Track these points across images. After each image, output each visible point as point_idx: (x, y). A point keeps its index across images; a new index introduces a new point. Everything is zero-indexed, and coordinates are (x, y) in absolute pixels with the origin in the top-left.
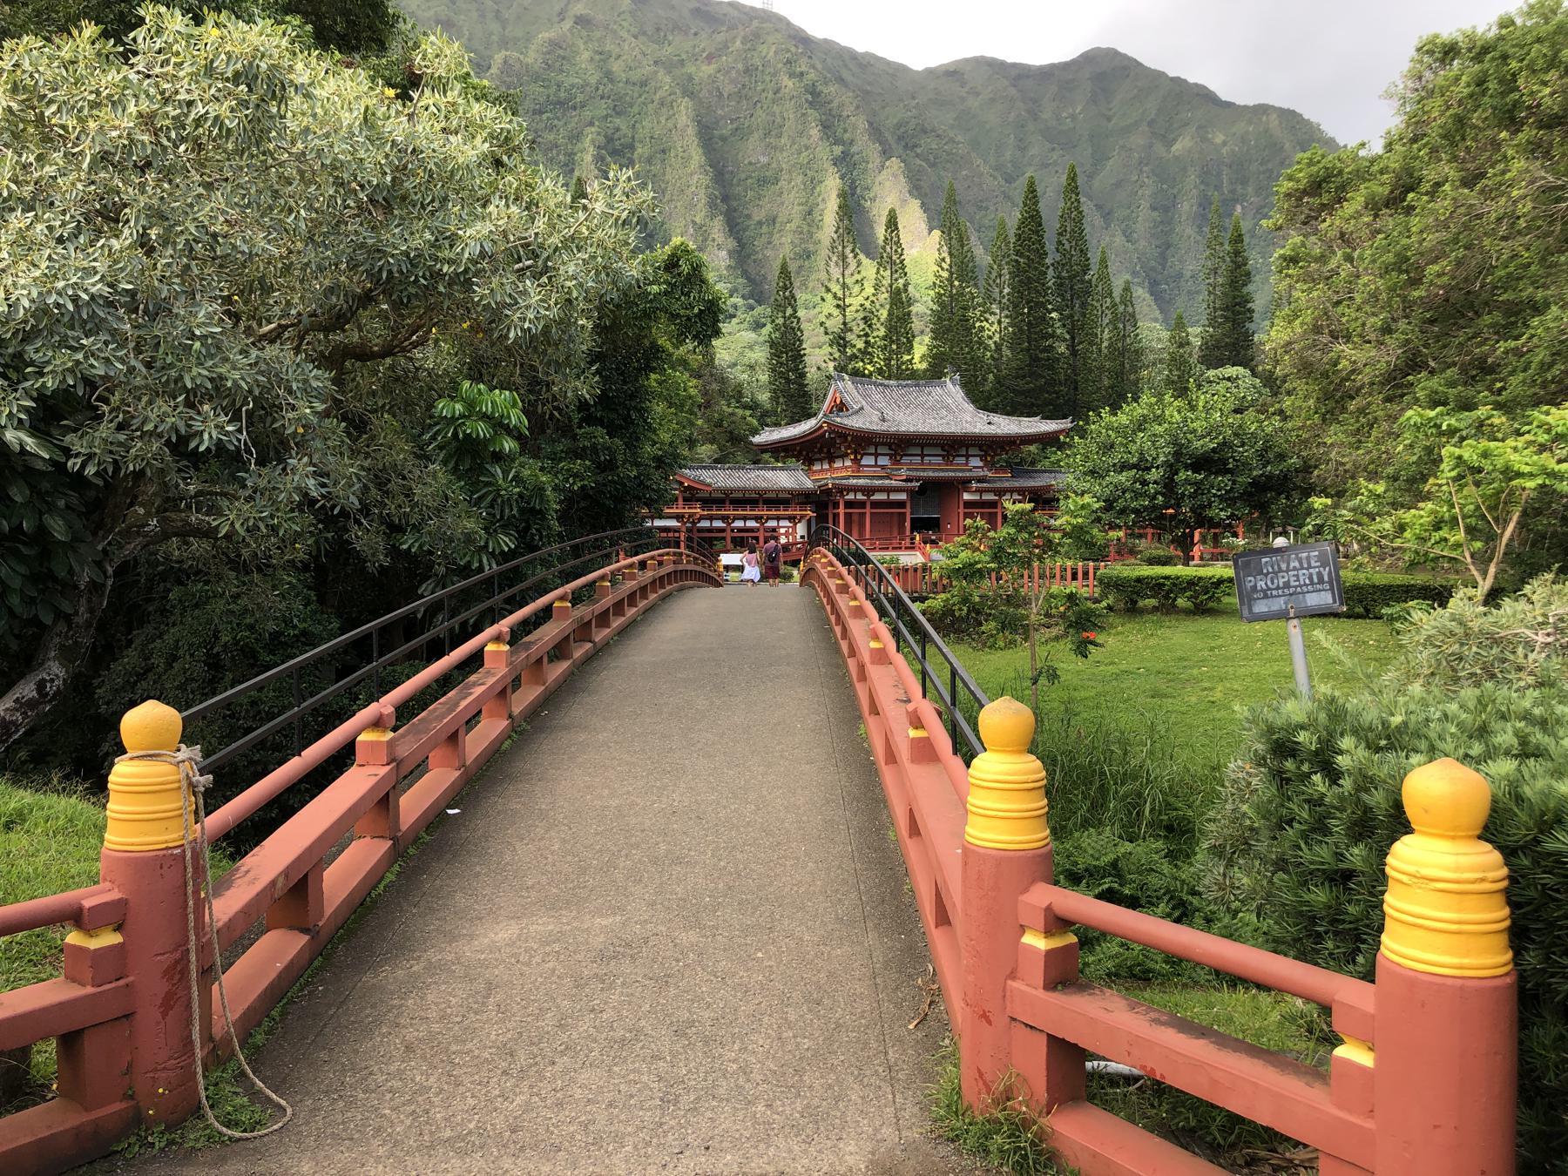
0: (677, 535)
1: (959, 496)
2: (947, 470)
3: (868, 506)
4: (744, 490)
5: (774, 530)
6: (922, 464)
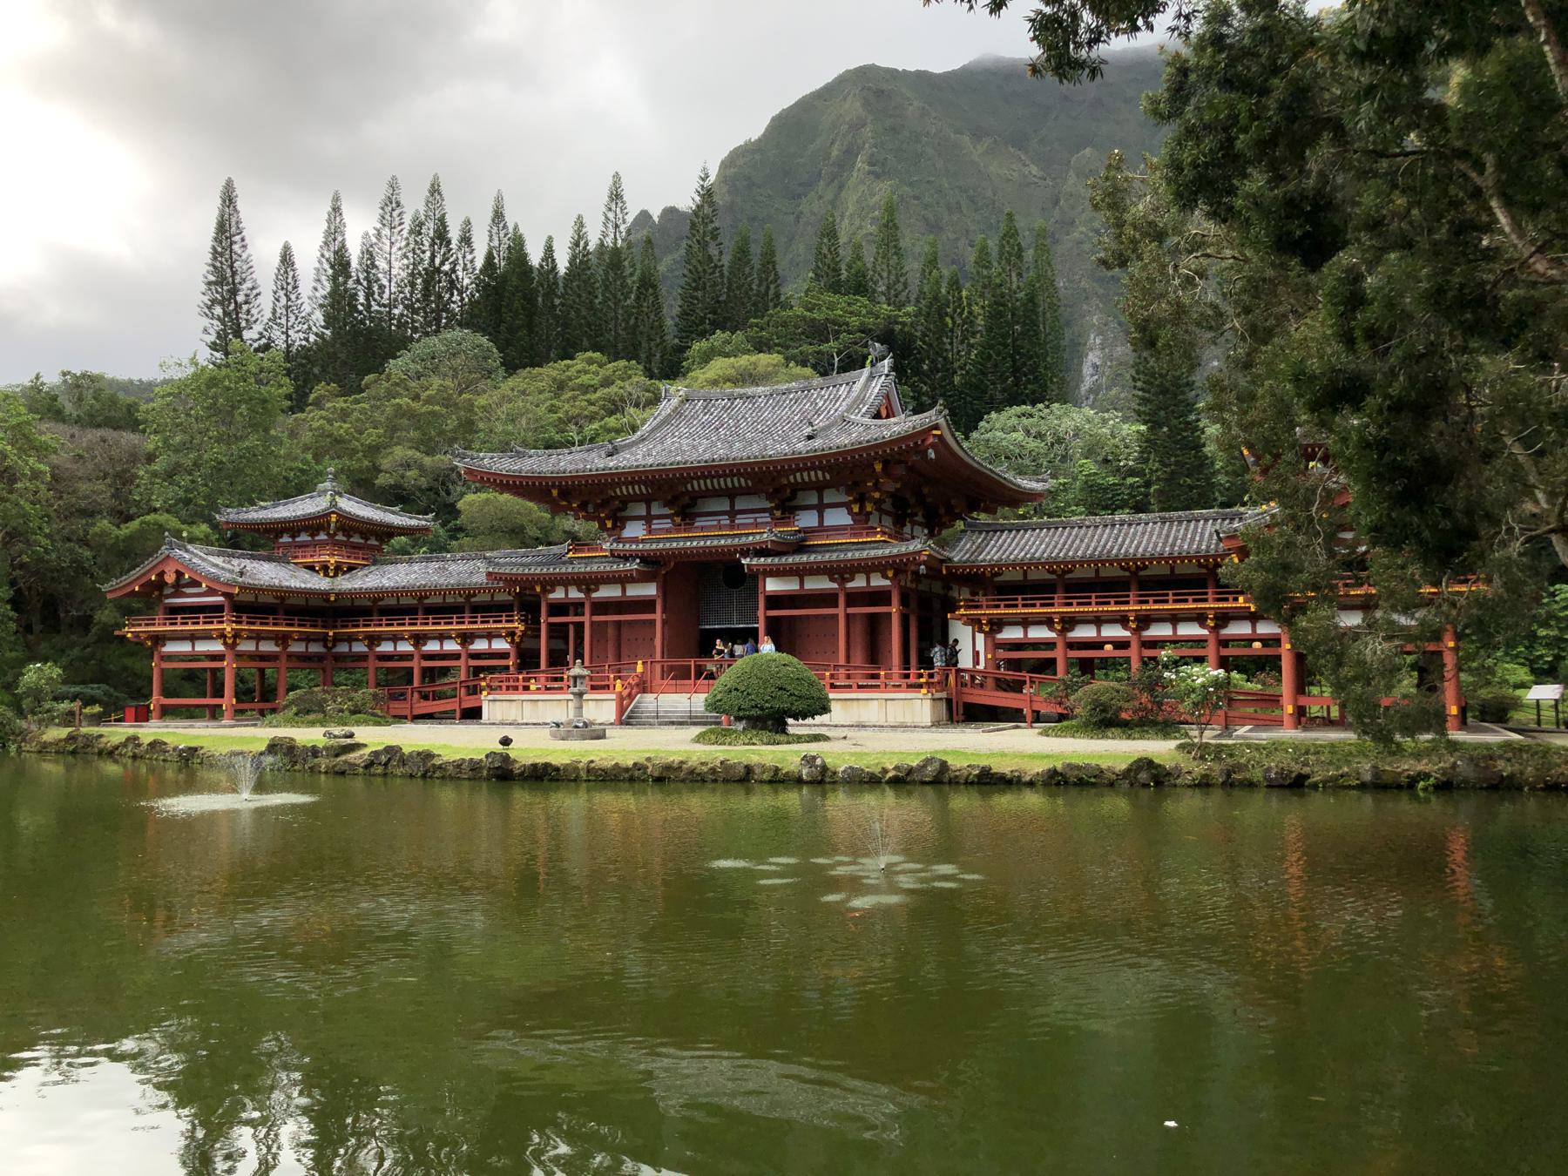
2: (691, 539)
6: (732, 527)
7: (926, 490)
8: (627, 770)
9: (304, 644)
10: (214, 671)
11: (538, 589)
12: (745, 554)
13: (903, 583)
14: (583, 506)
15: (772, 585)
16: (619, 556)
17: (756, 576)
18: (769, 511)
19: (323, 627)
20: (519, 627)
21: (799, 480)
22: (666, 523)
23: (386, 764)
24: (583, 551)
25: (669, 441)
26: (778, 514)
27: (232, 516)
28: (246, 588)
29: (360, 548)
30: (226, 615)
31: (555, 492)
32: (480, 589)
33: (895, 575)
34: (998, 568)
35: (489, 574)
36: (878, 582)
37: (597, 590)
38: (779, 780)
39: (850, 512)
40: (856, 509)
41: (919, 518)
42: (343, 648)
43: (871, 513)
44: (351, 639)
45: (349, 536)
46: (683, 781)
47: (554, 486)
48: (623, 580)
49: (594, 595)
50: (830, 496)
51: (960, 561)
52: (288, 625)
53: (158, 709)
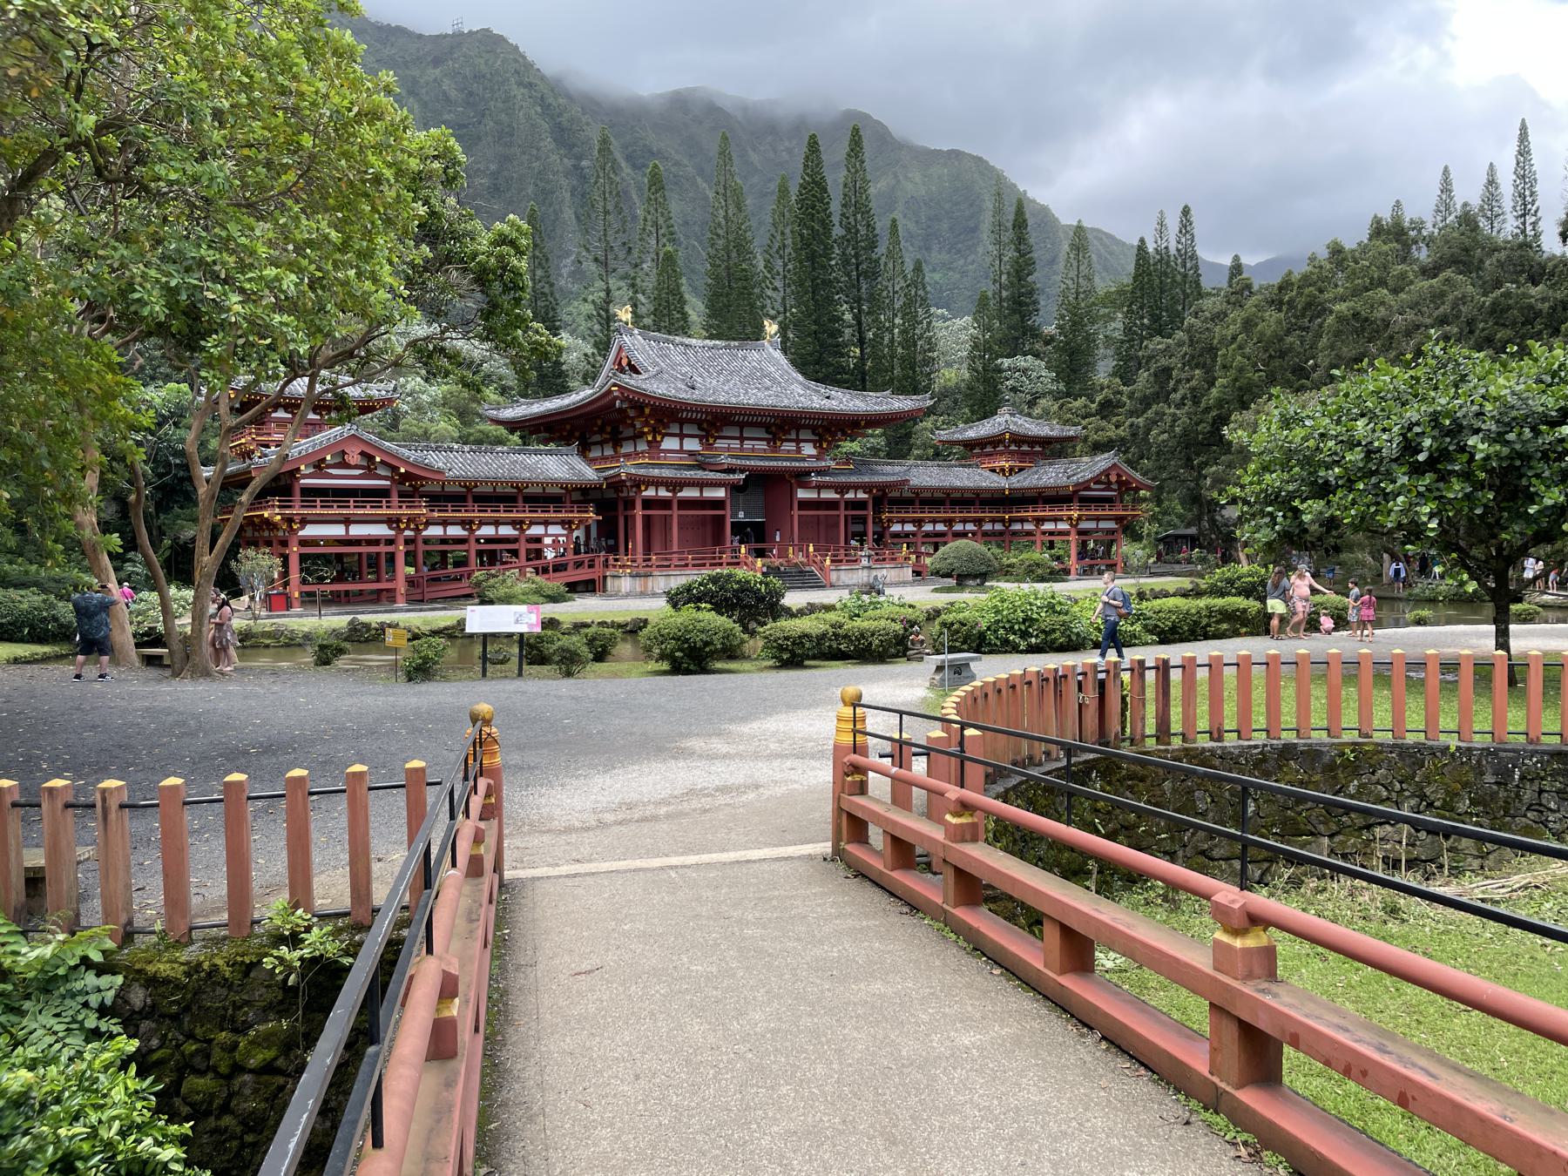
0: (390, 549)
1: (792, 494)
2: (776, 459)
3: (675, 506)
4: (495, 482)
5: (538, 540)
18: (768, 441)
24: (659, 459)
30: (395, 498)
36: (861, 495)
37: (681, 491)
48: (701, 484)
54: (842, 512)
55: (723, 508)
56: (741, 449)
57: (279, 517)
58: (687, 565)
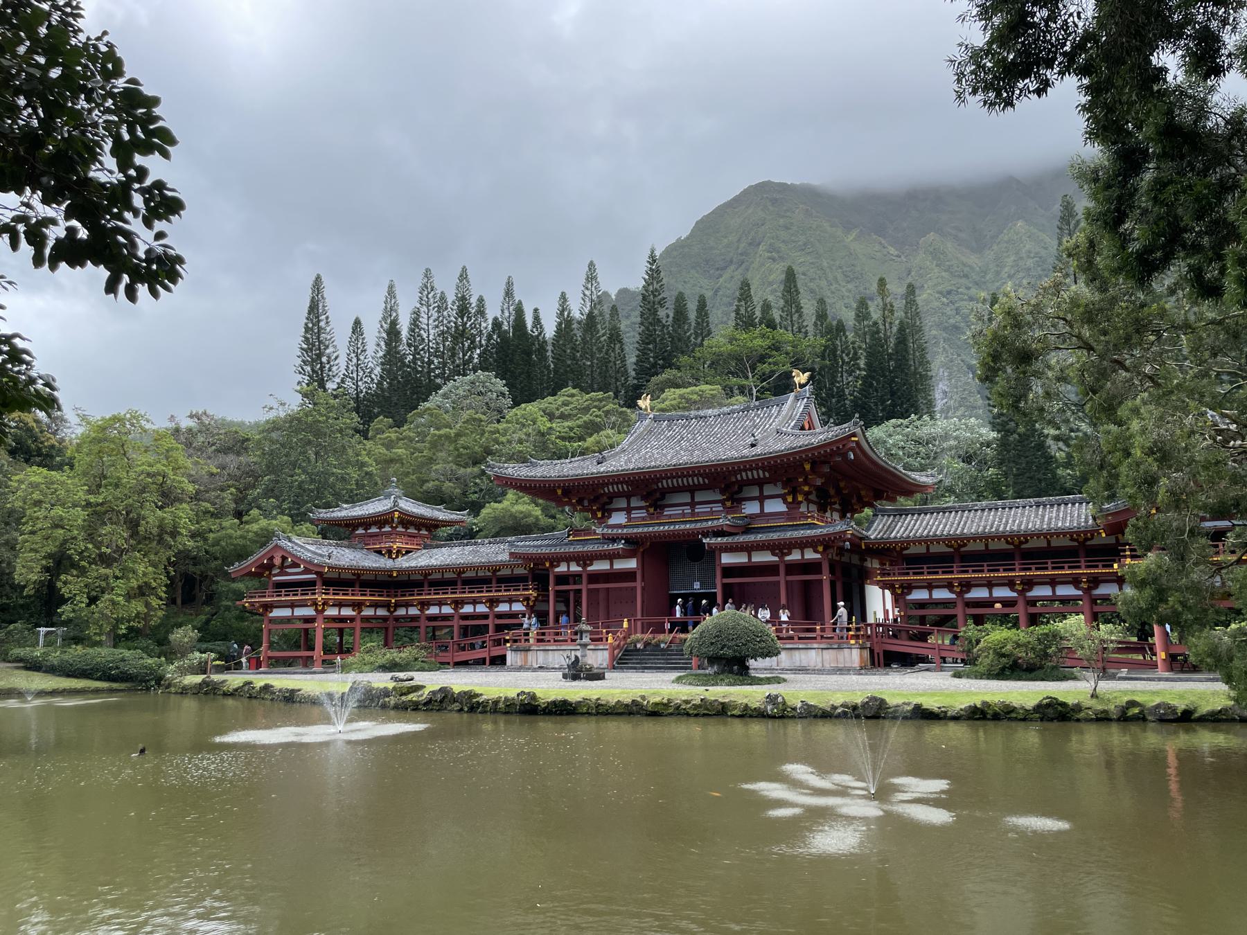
6: (693, 514)
7: (842, 484)
8: (627, 705)
9: (373, 609)
10: (306, 630)
11: (547, 565)
12: (706, 535)
13: (830, 556)
14: (580, 502)
15: (727, 559)
16: (608, 539)
17: (715, 552)
18: (722, 502)
19: (388, 596)
20: (532, 593)
21: (745, 478)
22: (643, 513)
23: (441, 701)
24: (581, 536)
25: (644, 452)
26: (729, 504)
27: (321, 515)
28: (333, 568)
29: (414, 537)
30: (318, 588)
31: (559, 492)
32: (503, 565)
33: (825, 549)
34: (907, 542)
35: (511, 554)
36: (810, 555)
38: (749, 714)
39: (785, 501)
40: (790, 499)
41: (837, 506)
42: (401, 612)
43: (801, 502)
44: (407, 605)
45: (407, 528)
46: (671, 714)
47: (559, 487)
48: (611, 557)
49: (589, 568)
50: (769, 490)
51: (876, 539)
52: (362, 595)
53: (266, 658)
54: (782, 578)
55: (635, 581)
56: (693, 514)
57: (247, 605)
58: (566, 641)
